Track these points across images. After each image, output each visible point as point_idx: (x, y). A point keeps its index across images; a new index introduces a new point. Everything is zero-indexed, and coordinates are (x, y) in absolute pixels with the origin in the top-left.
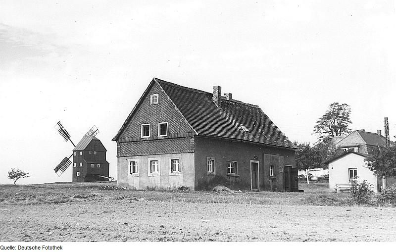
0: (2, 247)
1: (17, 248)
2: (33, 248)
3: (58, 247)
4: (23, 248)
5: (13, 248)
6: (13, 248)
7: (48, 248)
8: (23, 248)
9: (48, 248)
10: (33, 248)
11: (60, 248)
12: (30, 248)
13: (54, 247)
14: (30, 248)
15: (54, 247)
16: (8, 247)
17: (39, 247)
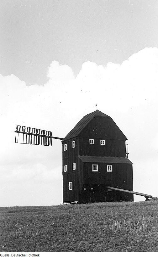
0: (1, 255)
1: (11, 255)
2: (21, 256)
3: (37, 255)
4: (14, 255)
5: (8, 255)
6: (8, 255)
7: (31, 255)
8: (14, 255)
9: (31, 255)
10: (21, 256)
12: (19, 256)
13: (34, 255)
14: (19, 256)
15: (34, 255)
16: (5, 255)
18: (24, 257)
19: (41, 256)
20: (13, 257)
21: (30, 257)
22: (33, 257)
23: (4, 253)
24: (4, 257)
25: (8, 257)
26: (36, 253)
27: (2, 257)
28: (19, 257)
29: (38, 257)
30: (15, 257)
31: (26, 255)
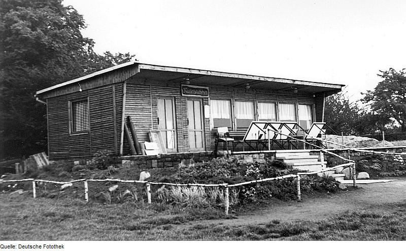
0: (2, 246)
1: (17, 247)
2: (34, 247)
3: (60, 246)
4: (23, 247)
5: (13, 247)
6: (13, 247)
9: (50, 247)
10: (34, 247)
12: (31, 247)
13: (55, 246)
14: (31, 247)
16: (9, 246)
17: (40, 246)
18: (39, 249)
19: (66, 248)
20: (22, 249)
21: (49, 249)
22: (54, 249)
23: (7, 243)
24: (7, 249)
25: (12, 249)
26: (59, 243)
27: (4, 249)
28: (30, 250)
29: (62, 249)
30: (25, 249)
31: (42, 247)
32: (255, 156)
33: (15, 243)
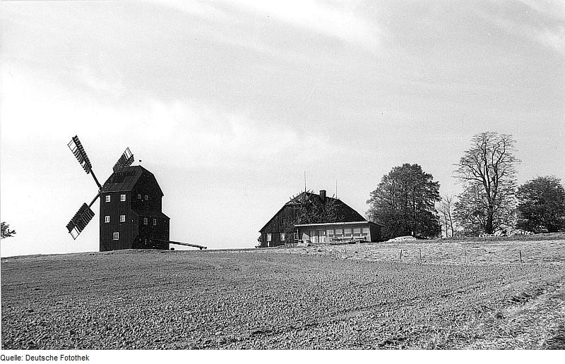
0: (3, 358)
1: (24, 358)
2: (48, 358)
3: (83, 357)
4: (32, 358)
5: (18, 358)
6: (18, 358)
7: (69, 358)
8: (32, 358)
10: (48, 358)
11: (85, 358)
12: (43, 358)
13: (77, 358)
14: (43, 358)
15: (77, 358)
16: (12, 357)
26: (82, 353)
31: (59, 358)
32: (339, 232)
33: (19, 353)
